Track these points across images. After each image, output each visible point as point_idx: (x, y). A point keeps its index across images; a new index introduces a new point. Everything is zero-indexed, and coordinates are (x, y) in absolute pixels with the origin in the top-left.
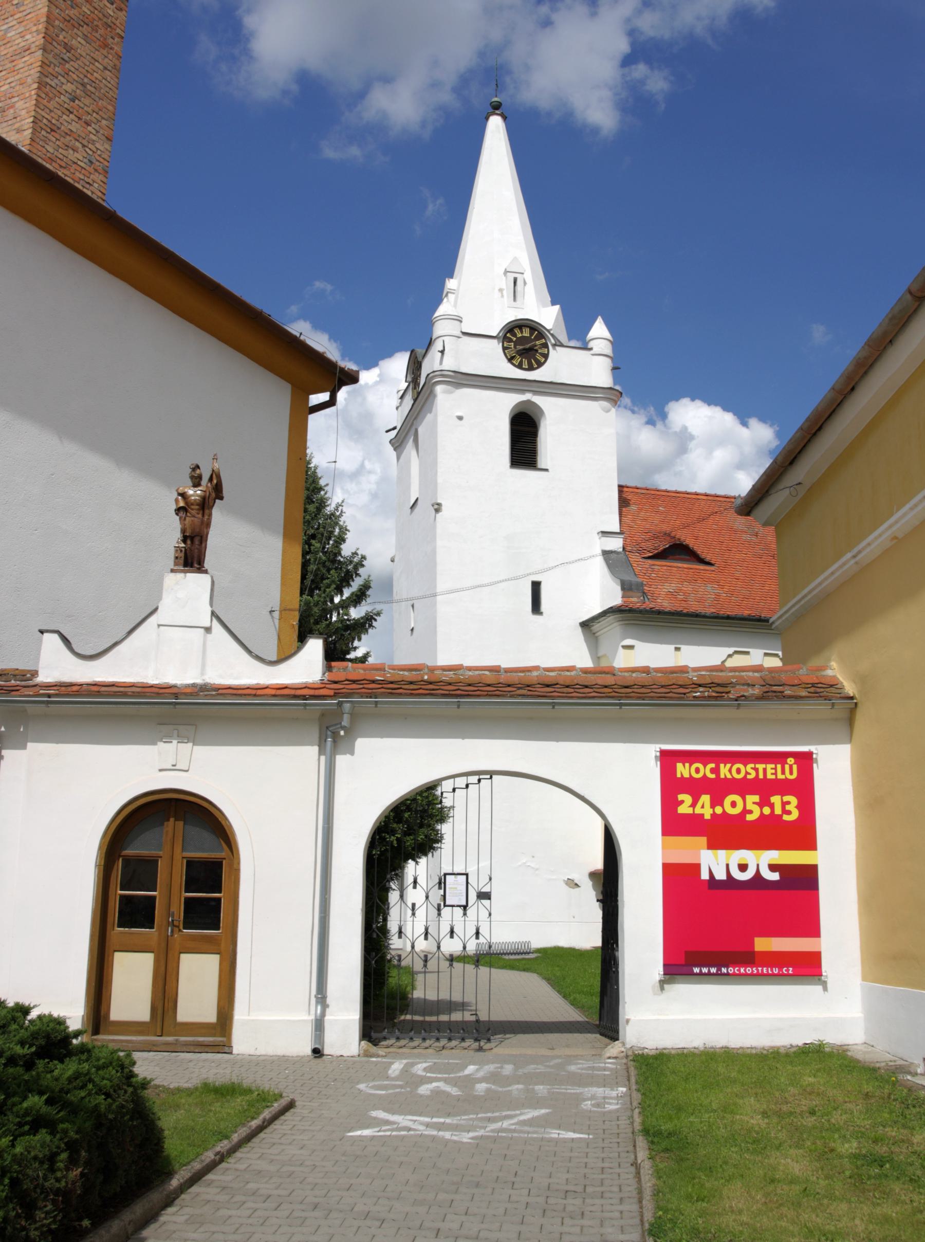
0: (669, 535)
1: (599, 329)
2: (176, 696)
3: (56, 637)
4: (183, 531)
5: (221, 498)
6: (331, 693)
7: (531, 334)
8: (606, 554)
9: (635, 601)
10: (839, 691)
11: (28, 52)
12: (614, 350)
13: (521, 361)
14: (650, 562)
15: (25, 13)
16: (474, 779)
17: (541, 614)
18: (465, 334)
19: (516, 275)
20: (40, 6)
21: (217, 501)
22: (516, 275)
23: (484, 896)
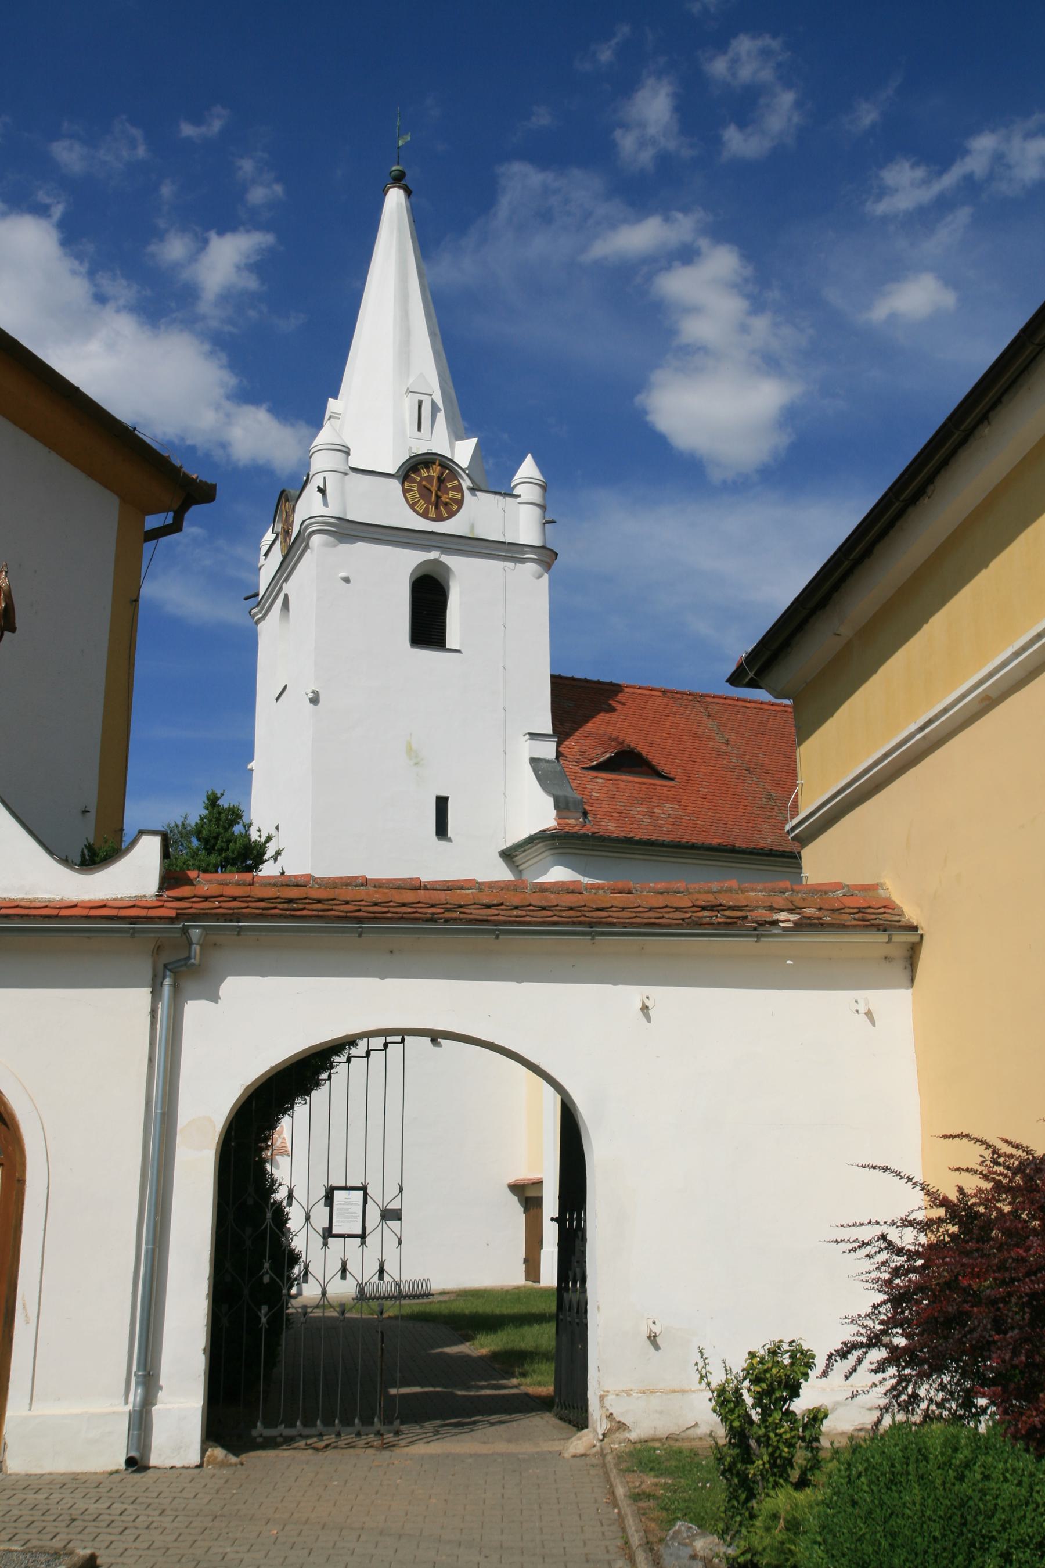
0: (616, 740)
1: (528, 469)
5: (13, 630)
6: (173, 913)
8: (534, 761)
9: (574, 824)
10: (897, 918)
12: (544, 498)
13: (427, 509)
14: (594, 774)
16: (377, 1042)
17: (449, 840)
18: (352, 469)
19: (421, 397)
21: (6, 633)
22: (421, 397)
23: (390, 1215)
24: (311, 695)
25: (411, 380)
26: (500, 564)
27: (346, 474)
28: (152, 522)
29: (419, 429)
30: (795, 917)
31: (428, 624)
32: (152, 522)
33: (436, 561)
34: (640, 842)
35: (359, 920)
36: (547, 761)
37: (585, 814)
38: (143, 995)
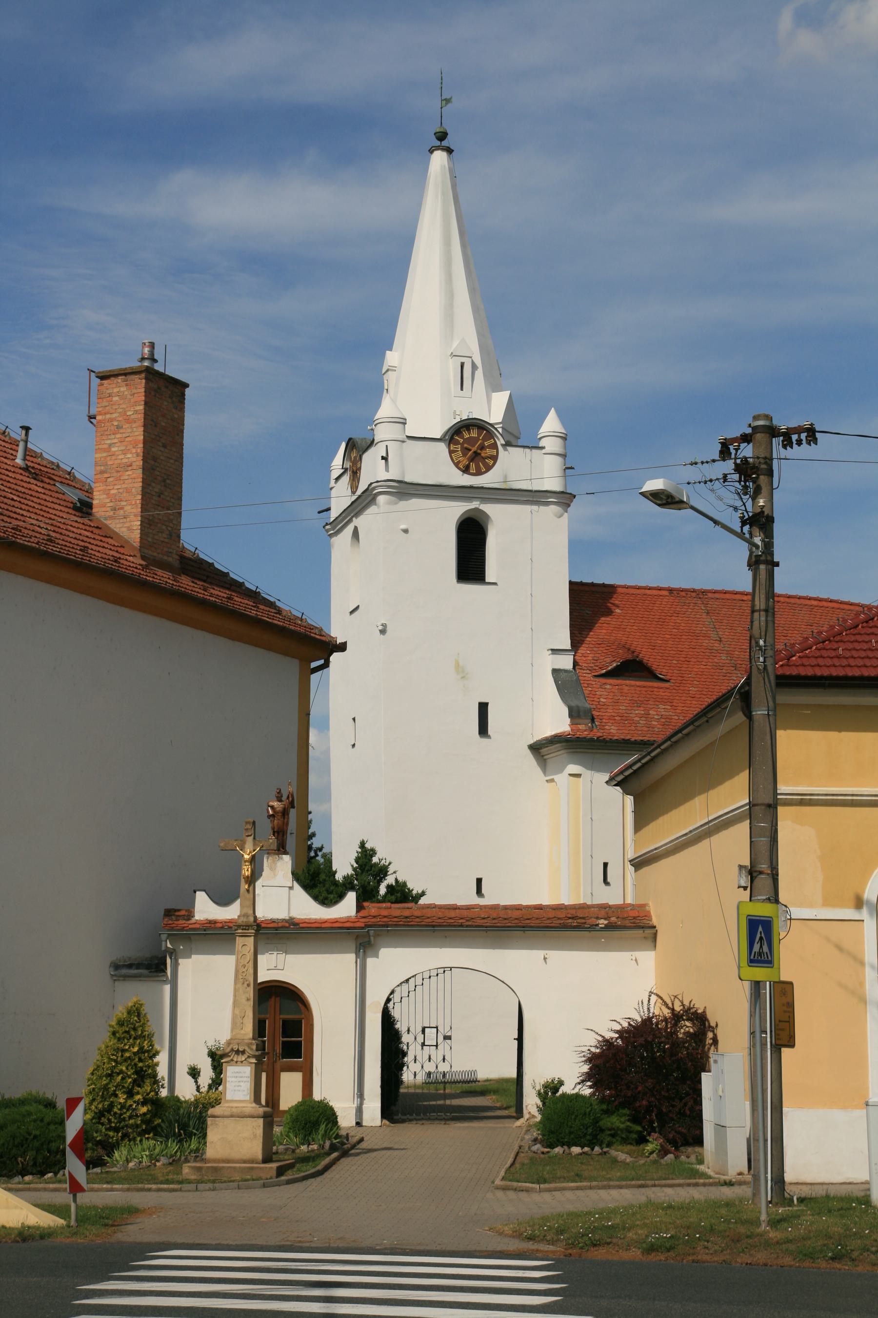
1: (551, 424)
2: (276, 929)
3: (204, 893)
4: (273, 828)
6: (363, 925)
7: (479, 435)
8: (555, 671)
9: (584, 730)
11: (130, 468)
12: (565, 448)
14: (603, 680)
15: (124, 435)
17: (489, 737)
18: (408, 437)
20: (136, 434)
23: (447, 1038)
24: (381, 628)
25: (456, 343)
26: (528, 508)
27: (403, 442)
28: (314, 665)
29: (462, 389)
30: (606, 922)
31: (471, 564)
32: (314, 665)
33: (477, 510)
34: (636, 742)
35: (434, 926)
36: (566, 671)
37: (593, 720)
38: (352, 956)
